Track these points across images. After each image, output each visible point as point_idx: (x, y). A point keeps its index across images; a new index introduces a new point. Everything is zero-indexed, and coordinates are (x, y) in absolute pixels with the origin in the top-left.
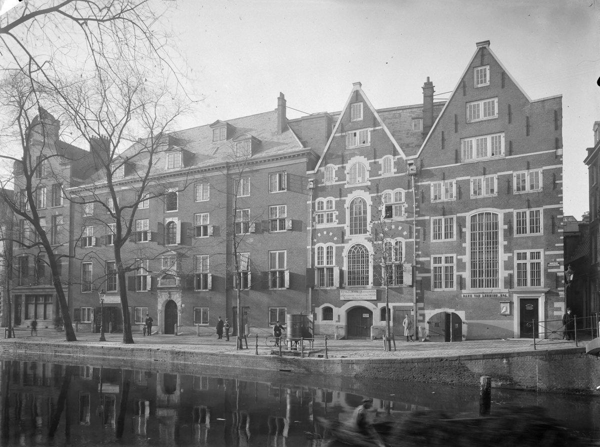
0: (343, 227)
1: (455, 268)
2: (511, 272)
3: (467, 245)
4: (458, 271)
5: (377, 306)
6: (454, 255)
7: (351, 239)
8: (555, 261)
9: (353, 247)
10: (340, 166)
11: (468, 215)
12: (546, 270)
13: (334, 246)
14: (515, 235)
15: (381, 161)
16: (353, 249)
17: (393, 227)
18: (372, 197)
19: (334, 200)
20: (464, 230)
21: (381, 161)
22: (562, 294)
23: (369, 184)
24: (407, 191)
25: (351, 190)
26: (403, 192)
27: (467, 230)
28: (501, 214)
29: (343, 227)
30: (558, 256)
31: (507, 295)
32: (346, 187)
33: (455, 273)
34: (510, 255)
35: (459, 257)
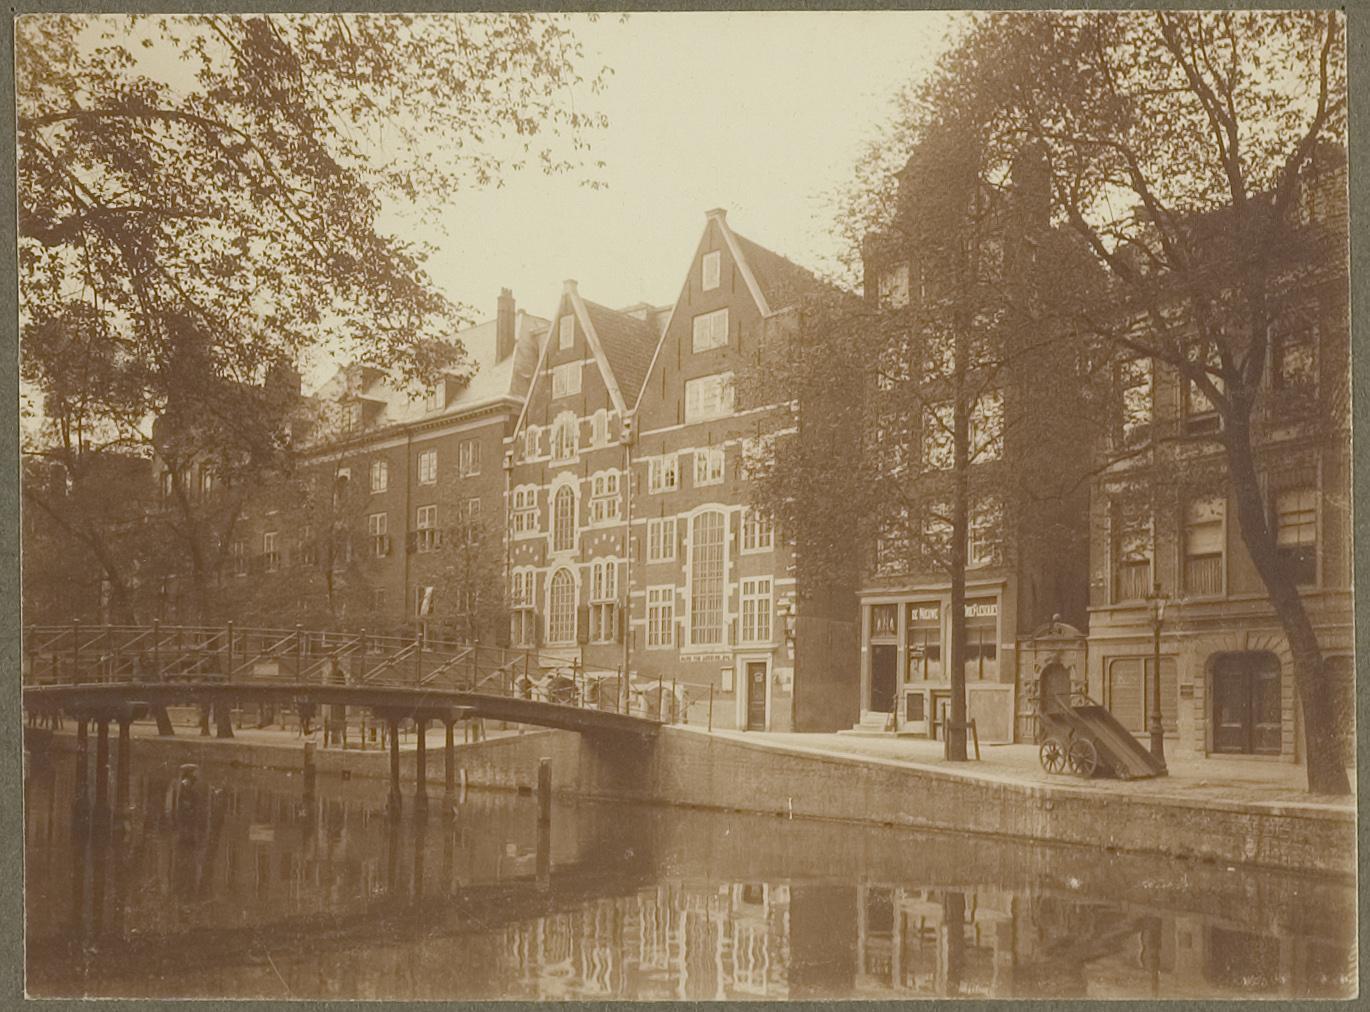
1: (673, 609)
2: (735, 615)
3: (688, 569)
4: (676, 615)
6: (672, 586)
8: (785, 597)
11: (690, 516)
12: (775, 612)
14: (743, 552)
20: (685, 542)
22: (791, 655)
27: (688, 542)
30: (787, 588)
31: (731, 656)
32: (551, 465)
33: (674, 619)
34: (735, 585)
35: (679, 590)
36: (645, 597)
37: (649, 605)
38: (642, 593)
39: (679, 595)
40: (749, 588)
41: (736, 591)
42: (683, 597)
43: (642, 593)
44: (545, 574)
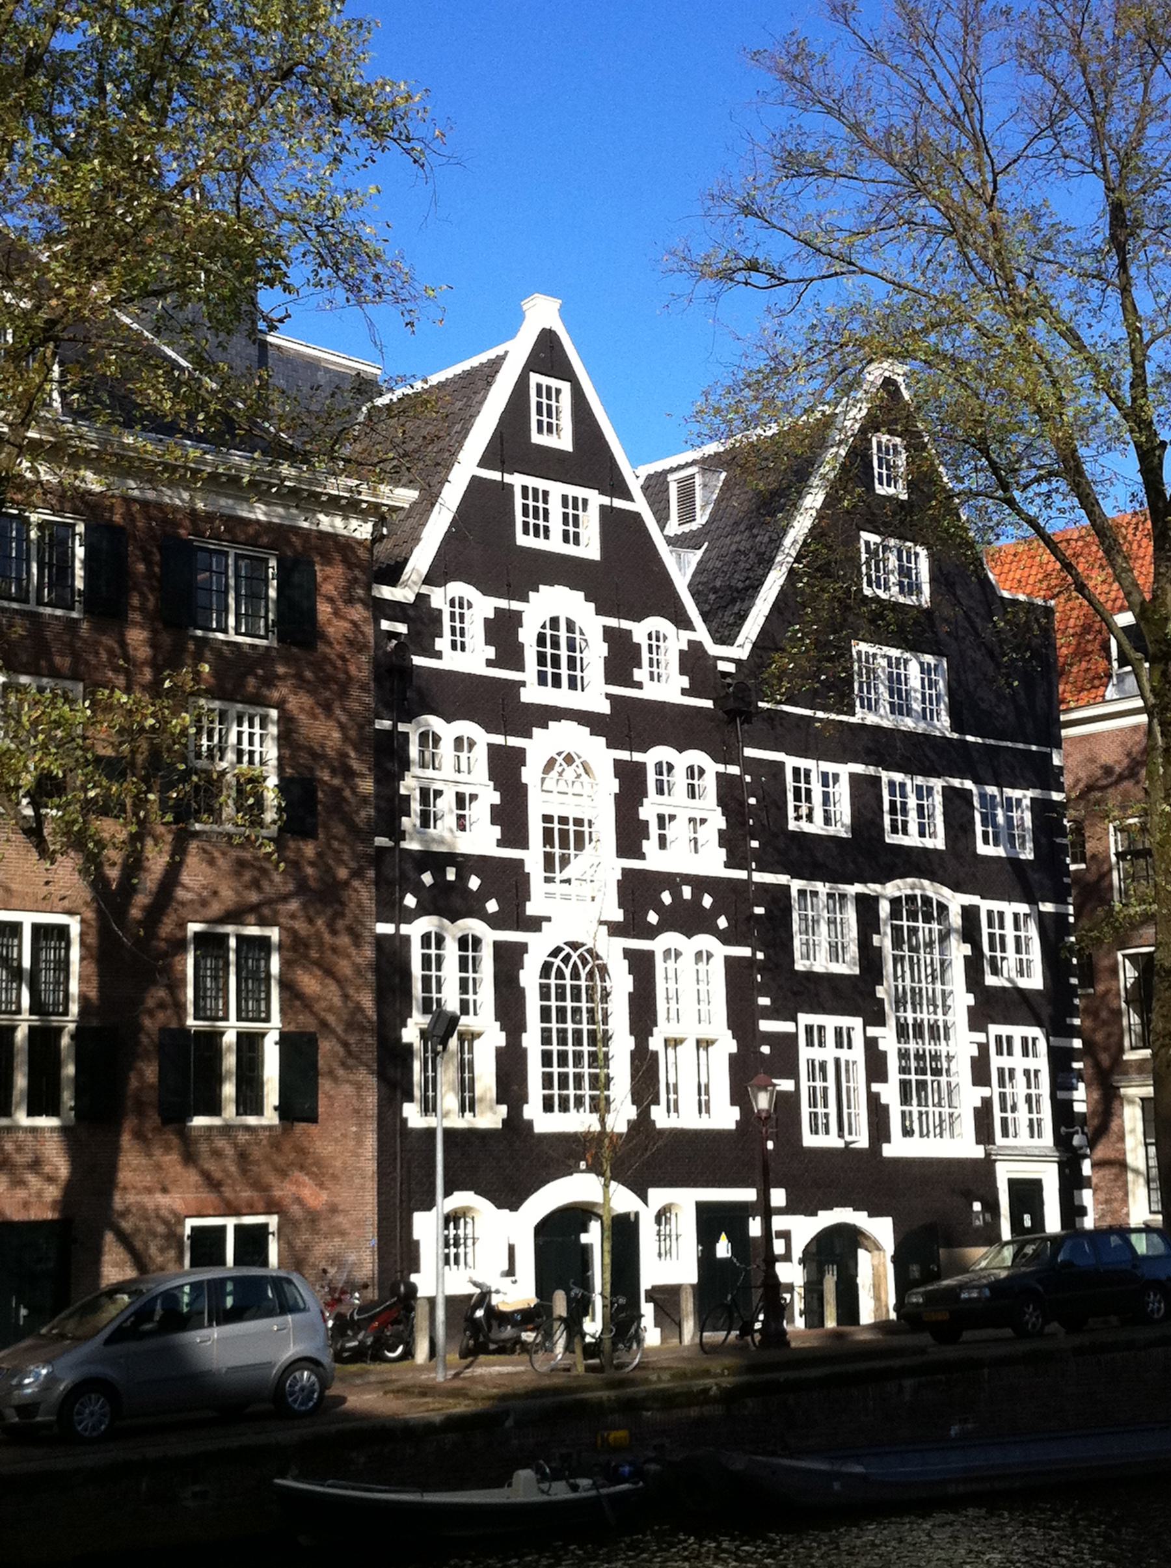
0: (521, 862)
5: (644, 1199)
6: (857, 1022)
7: (548, 919)
9: (555, 953)
10: (503, 603)
13: (489, 936)
15: (640, 631)
16: (557, 962)
17: (687, 892)
18: (618, 763)
19: (483, 738)
20: (876, 940)
21: (640, 631)
23: (605, 708)
24: (721, 768)
25: (546, 715)
26: (712, 768)
28: (956, 901)
29: (521, 862)
34: (980, 1037)
35: (872, 1031)
36: (795, 1036)
37: (805, 1053)
38: (786, 1027)
39: (871, 1044)
40: (1004, 1045)
41: (983, 1048)
42: (882, 1046)
43: (786, 1027)
44: (523, 948)
